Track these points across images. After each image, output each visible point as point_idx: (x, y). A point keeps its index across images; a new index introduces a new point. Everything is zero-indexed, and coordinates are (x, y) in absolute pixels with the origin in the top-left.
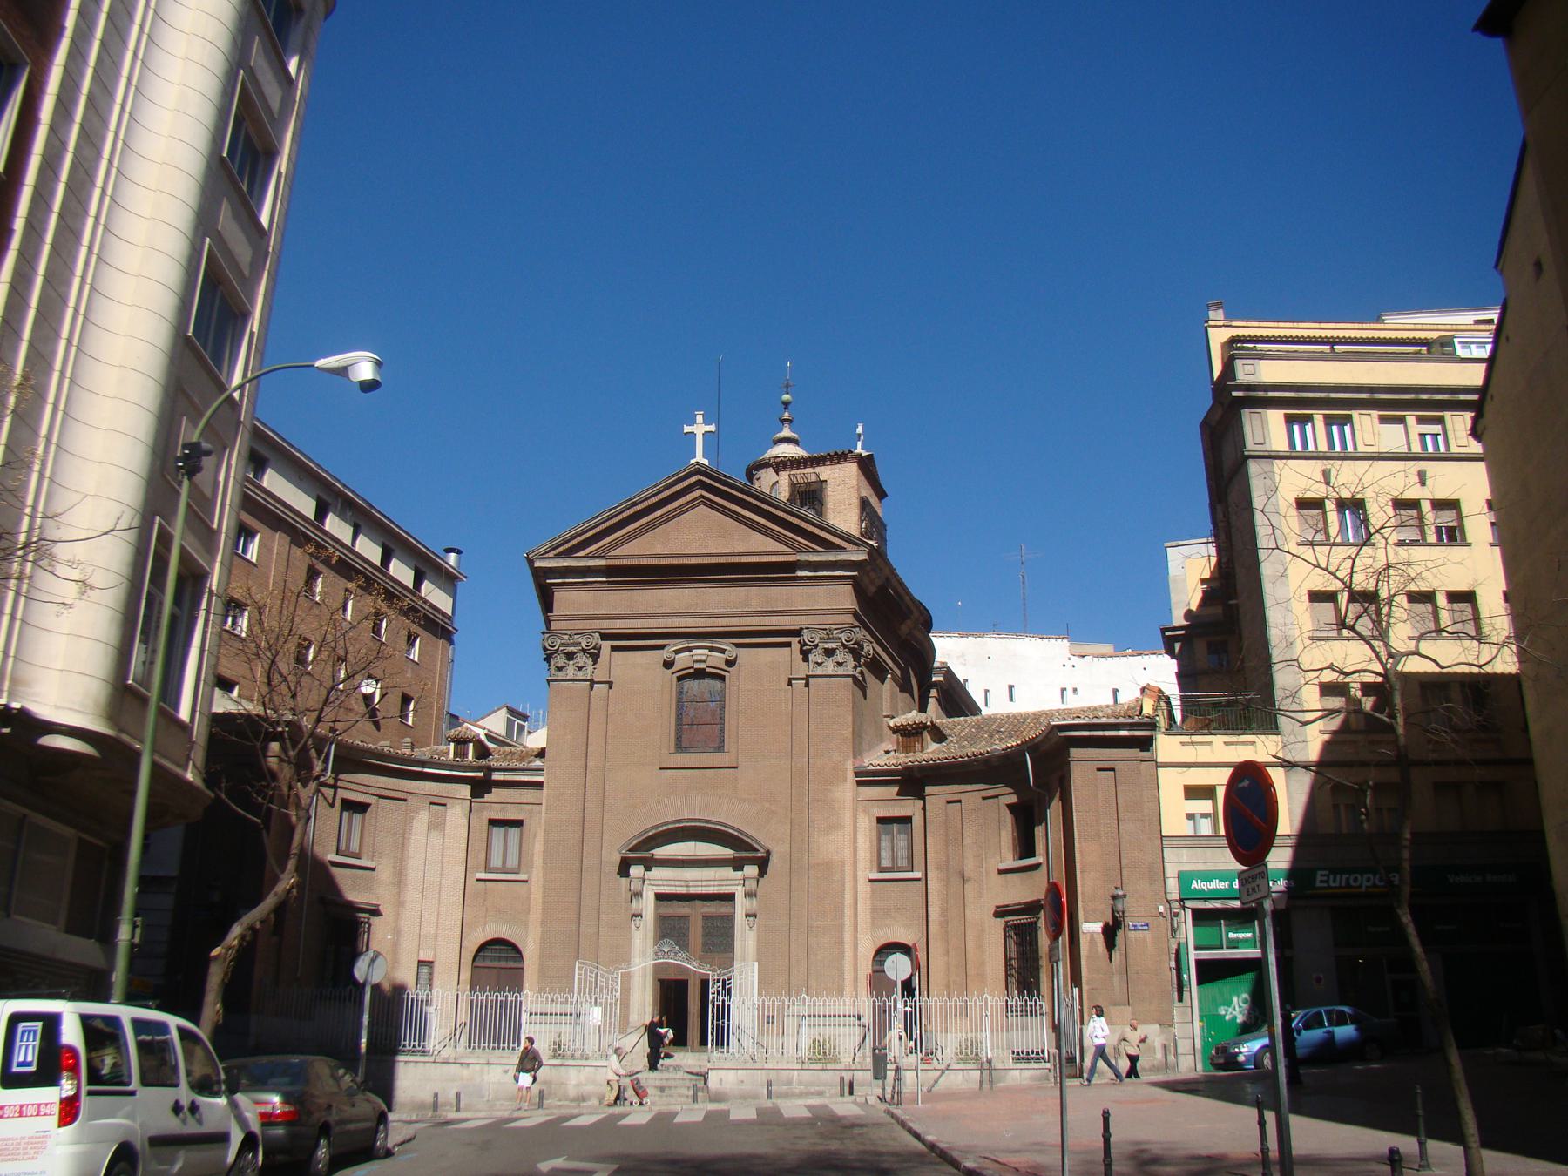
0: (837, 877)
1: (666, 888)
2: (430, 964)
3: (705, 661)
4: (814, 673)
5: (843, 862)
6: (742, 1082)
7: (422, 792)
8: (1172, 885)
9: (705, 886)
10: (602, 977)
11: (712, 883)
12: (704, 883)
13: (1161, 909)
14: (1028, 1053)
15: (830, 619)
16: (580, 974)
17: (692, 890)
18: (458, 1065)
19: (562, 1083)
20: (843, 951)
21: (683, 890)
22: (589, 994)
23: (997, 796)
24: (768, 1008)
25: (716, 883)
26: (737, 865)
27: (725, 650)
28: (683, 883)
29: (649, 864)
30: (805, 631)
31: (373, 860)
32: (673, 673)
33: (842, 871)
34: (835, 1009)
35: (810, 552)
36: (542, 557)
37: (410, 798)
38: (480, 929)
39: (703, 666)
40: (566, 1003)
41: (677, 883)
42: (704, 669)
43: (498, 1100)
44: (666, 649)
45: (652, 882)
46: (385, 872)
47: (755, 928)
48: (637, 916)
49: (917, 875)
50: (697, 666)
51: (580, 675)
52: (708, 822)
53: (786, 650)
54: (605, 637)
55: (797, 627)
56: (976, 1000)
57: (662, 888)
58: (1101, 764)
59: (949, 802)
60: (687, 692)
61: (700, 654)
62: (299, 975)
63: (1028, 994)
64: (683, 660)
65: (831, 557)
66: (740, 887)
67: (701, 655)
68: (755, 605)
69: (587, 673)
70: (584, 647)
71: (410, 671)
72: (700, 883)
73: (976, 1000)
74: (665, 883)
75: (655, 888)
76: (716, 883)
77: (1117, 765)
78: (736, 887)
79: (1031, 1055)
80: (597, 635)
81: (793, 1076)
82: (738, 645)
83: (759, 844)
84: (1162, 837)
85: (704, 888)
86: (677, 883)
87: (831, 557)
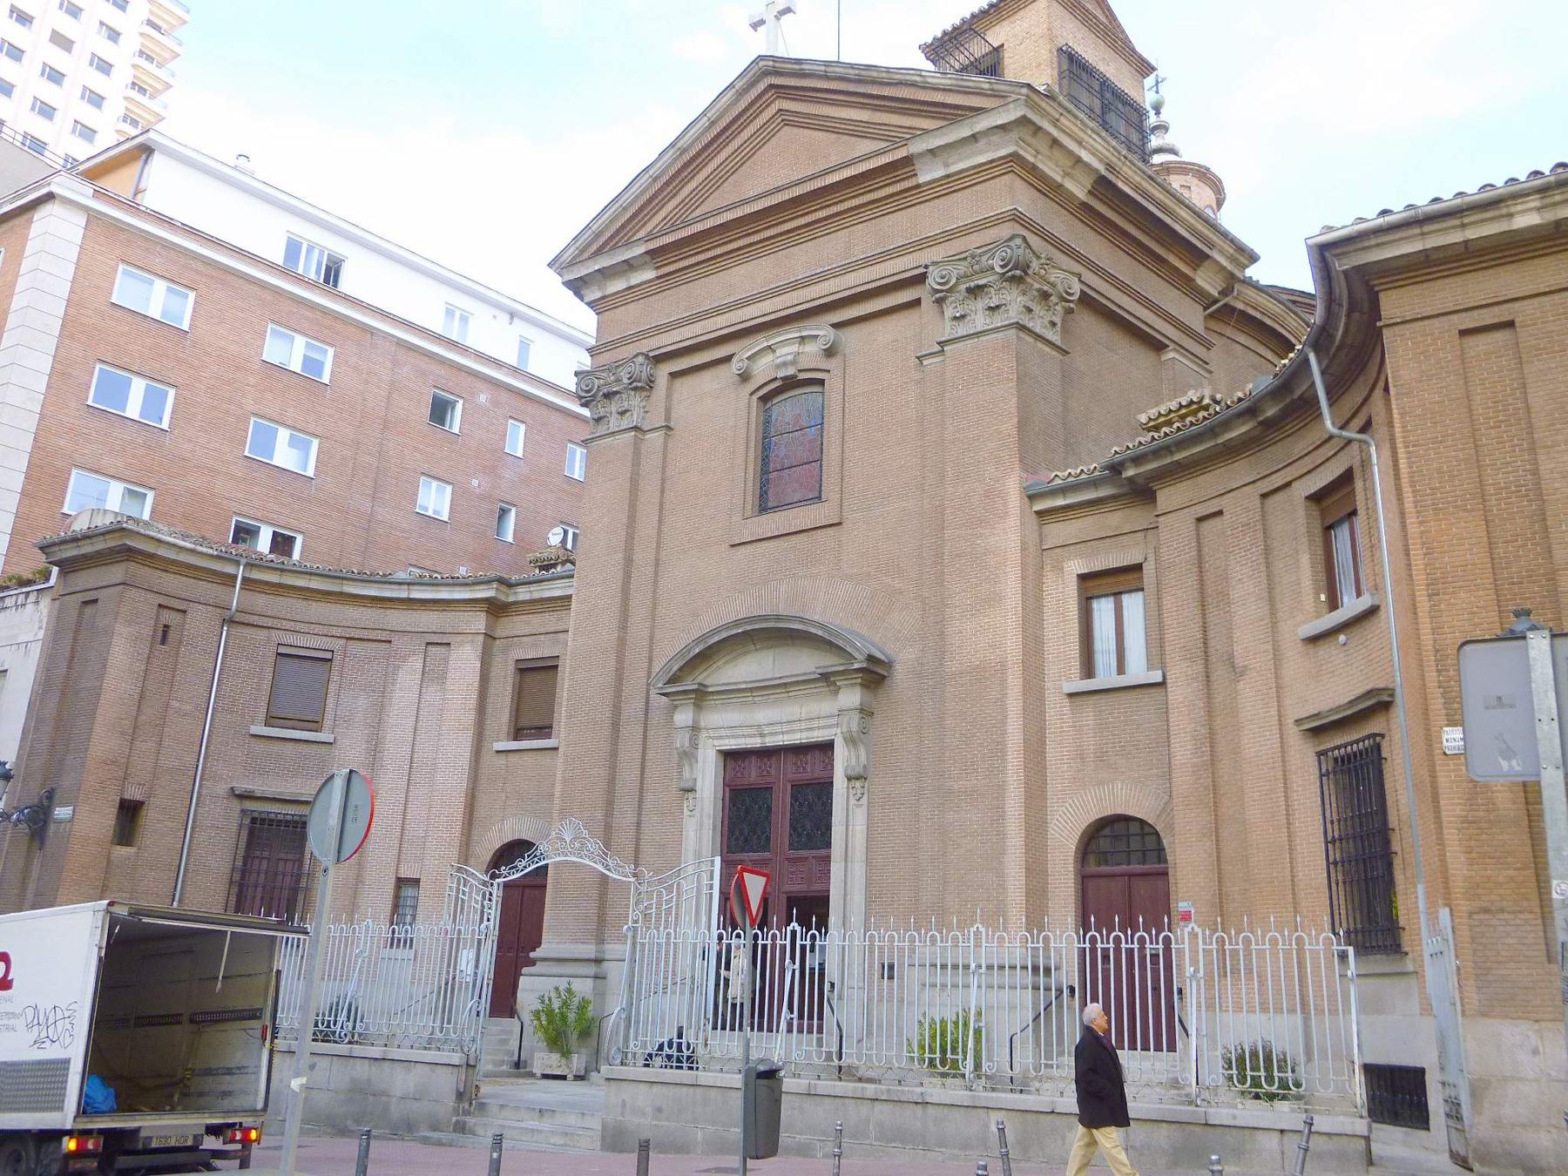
5: (1003, 666)
6: (659, 1110)
9: (788, 732)
11: (796, 726)
20: (1002, 836)
21: (755, 743)
23: (1288, 485)
28: (753, 731)
32: (751, 394)
33: (1003, 682)
37: (395, 638)
38: (495, 828)
39: (791, 371)
42: (793, 377)
44: (735, 360)
50: (781, 374)
56: (872, 936)
58: (1469, 321)
63: (1250, 923)
64: (764, 369)
65: (964, 131)
75: (716, 742)
78: (834, 731)
80: (640, 359)
85: (786, 737)
87: (964, 131)
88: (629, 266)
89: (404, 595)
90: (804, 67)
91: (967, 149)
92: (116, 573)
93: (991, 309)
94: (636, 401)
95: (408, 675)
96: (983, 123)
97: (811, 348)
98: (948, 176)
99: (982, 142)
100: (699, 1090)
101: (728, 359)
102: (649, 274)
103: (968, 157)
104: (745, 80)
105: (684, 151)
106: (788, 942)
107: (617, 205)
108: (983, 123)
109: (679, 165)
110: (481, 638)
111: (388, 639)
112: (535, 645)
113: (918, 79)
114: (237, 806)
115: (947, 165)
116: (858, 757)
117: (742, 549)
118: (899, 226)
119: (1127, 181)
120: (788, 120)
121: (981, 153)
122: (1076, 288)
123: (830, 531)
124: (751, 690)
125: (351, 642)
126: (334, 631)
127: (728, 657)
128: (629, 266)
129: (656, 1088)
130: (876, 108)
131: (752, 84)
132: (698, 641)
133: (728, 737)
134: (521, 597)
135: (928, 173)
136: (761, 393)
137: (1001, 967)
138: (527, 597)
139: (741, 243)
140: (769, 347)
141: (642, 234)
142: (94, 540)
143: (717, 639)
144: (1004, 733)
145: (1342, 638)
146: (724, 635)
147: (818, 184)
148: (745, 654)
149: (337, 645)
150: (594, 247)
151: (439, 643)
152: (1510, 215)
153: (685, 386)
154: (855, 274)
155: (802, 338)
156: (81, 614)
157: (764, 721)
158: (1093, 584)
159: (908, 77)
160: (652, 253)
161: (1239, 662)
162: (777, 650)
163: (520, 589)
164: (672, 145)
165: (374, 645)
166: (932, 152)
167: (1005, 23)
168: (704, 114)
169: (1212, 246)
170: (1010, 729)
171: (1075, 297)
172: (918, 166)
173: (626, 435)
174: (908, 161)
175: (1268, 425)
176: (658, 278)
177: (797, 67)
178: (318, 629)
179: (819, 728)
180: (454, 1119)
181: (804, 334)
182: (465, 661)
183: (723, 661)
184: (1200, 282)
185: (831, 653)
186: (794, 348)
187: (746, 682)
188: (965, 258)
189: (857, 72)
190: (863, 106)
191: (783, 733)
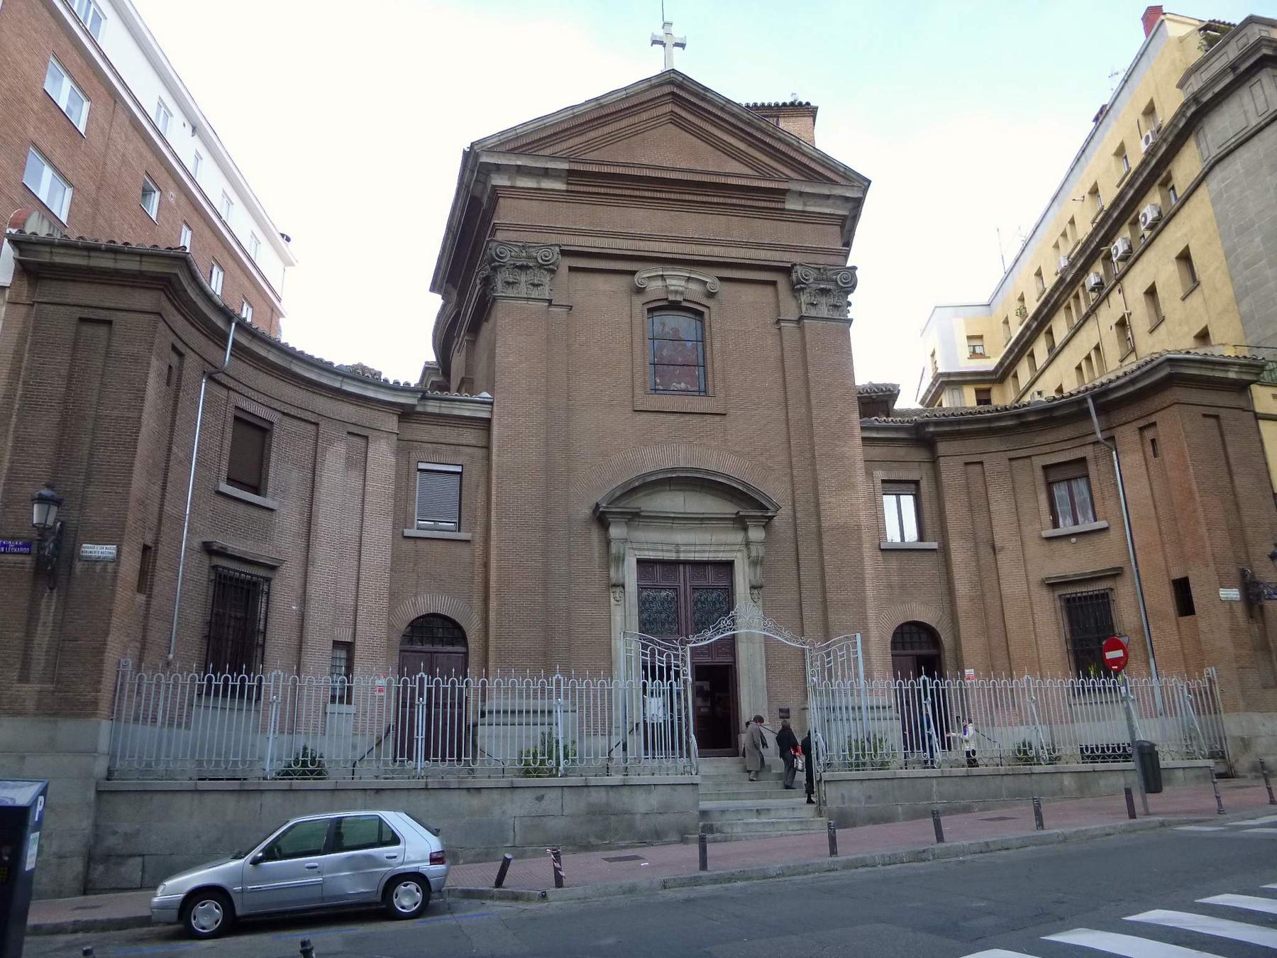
1: (651, 553)
2: (349, 647)
3: (682, 293)
6: (870, 797)
7: (338, 418)
9: (699, 552)
10: (661, 654)
11: (707, 548)
12: (698, 548)
14: (1103, 751)
17: (683, 556)
18: (465, 791)
21: (672, 556)
22: (676, 680)
23: (1029, 457)
26: (741, 523)
29: (634, 517)
30: (798, 267)
33: (860, 538)
36: (490, 151)
39: (679, 298)
40: (528, 697)
41: (665, 548)
43: (531, 844)
44: (637, 276)
47: (760, 603)
48: (615, 586)
49: (934, 545)
50: (671, 298)
51: (535, 293)
52: (707, 472)
53: (769, 290)
54: (564, 253)
57: (646, 553)
59: (967, 464)
61: (675, 284)
62: (171, 656)
64: (655, 288)
65: (825, 190)
66: (739, 555)
67: (677, 283)
68: (736, 236)
70: (540, 261)
72: (693, 548)
74: (649, 546)
75: (637, 553)
77: (1223, 413)
78: (735, 554)
79: (1108, 753)
80: (557, 249)
82: (721, 279)
83: (772, 504)
85: (696, 555)
87: (825, 190)
88: (546, 173)
89: (337, 385)
90: (708, 94)
91: (821, 202)
92: (145, 299)
94: (546, 278)
95: (335, 458)
96: (837, 191)
97: (694, 286)
98: (803, 212)
99: (830, 202)
100: (895, 781)
101: (633, 273)
102: (563, 187)
103: (819, 206)
104: (658, 80)
105: (602, 106)
106: (922, 687)
107: (541, 123)
109: (595, 115)
110: (395, 437)
113: (795, 143)
114: (206, 560)
115: (805, 205)
116: (755, 574)
117: (644, 416)
118: (765, 230)
120: (676, 121)
121: (828, 206)
123: (718, 418)
124: (674, 518)
125: (286, 418)
126: (276, 405)
127: (647, 492)
128: (546, 173)
130: (751, 145)
131: (660, 85)
132: (638, 478)
133: (648, 550)
134: (430, 409)
135: (792, 205)
138: (437, 411)
140: (662, 275)
141: (548, 152)
142: (120, 257)
143: (654, 478)
144: (863, 569)
145: (1073, 540)
146: (661, 476)
147: (723, 180)
148: (662, 491)
150: (512, 145)
151: (361, 435)
152: (1228, 371)
153: (581, 278)
155: (689, 278)
156: (77, 333)
157: (680, 542)
159: (789, 139)
160: (571, 172)
161: (998, 544)
162: (687, 493)
163: (431, 403)
164: (596, 99)
165: (303, 424)
166: (801, 194)
168: (625, 89)
172: (788, 197)
173: (541, 304)
174: (784, 192)
175: (1022, 424)
176: (567, 191)
177: (703, 92)
178: (264, 399)
179: (723, 551)
180: (701, 824)
181: (693, 276)
182: (382, 454)
183: (641, 494)
185: (731, 502)
186: (683, 283)
187: (674, 513)
189: (751, 118)
190: (743, 140)
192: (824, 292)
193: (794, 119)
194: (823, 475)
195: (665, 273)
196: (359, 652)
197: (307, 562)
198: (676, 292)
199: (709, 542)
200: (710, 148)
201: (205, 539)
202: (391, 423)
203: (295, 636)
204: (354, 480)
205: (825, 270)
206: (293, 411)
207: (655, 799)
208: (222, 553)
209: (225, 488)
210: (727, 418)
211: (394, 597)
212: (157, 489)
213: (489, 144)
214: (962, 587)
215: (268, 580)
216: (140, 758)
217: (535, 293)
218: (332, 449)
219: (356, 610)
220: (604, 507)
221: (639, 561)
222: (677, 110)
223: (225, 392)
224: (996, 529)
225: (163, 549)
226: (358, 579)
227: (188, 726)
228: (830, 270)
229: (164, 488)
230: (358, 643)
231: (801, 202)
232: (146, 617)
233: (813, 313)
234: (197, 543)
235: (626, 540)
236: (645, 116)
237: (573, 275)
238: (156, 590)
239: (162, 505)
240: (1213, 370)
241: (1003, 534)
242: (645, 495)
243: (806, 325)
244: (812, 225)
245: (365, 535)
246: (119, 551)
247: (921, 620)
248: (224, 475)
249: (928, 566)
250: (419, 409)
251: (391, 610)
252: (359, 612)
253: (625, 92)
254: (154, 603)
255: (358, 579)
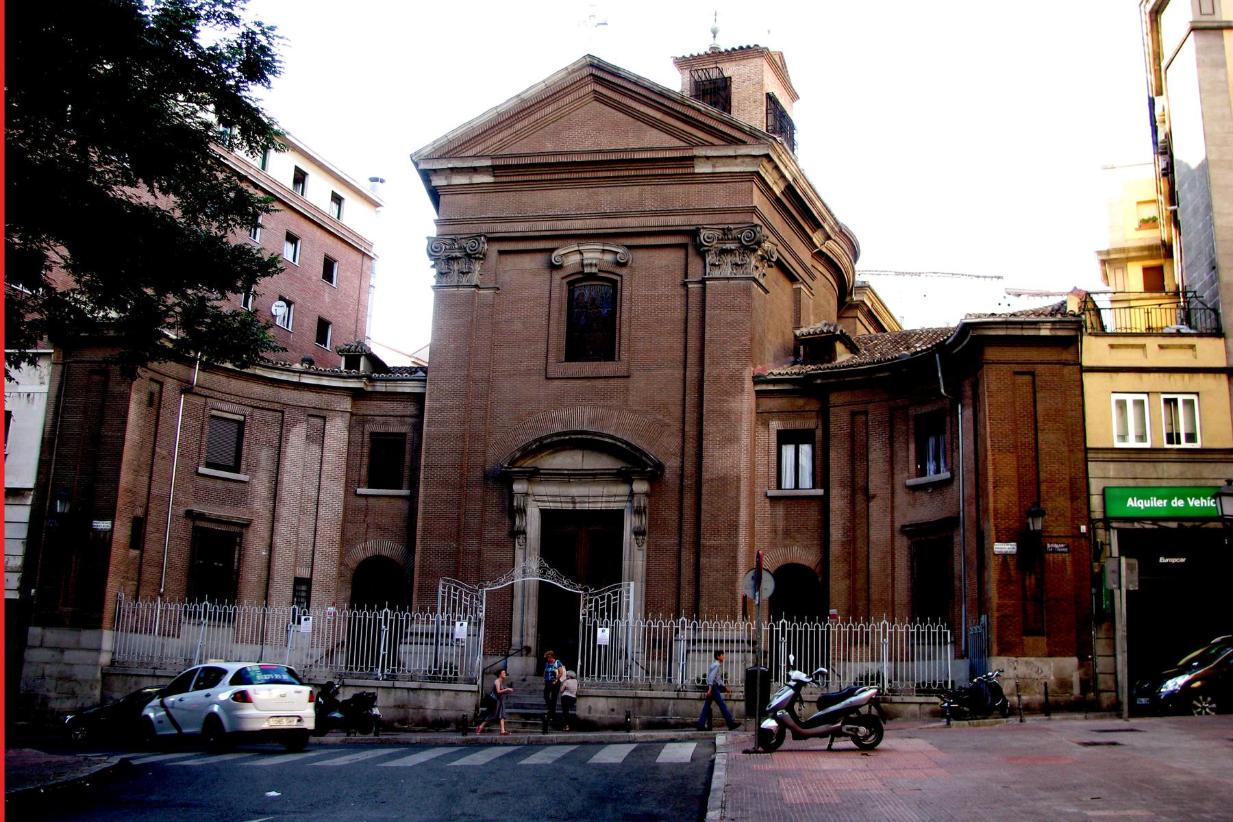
0: (732, 494)
1: (552, 504)
3: (596, 265)
4: (711, 276)
5: (738, 478)
6: (613, 710)
8: (1096, 501)
10: (466, 595)
11: (599, 499)
12: (591, 499)
13: (1083, 529)
15: (729, 218)
16: (444, 592)
19: (421, 708)
22: (442, 614)
24: (655, 633)
25: (604, 499)
26: (623, 477)
27: (617, 253)
28: (569, 499)
29: (534, 475)
31: (246, 474)
32: (563, 278)
33: (738, 488)
34: (727, 634)
35: (705, 145)
39: (594, 270)
41: (563, 499)
44: (555, 253)
45: (537, 498)
46: (261, 486)
47: (645, 547)
50: (587, 270)
51: (464, 281)
54: (490, 240)
55: (694, 228)
57: (548, 504)
60: (578, 298)
62: (162, 590)
68: (649, 204)
69: (475, 278)
71: (327, 295)
72: (587, 500)
73: (695, 624)
74: (550, 498)
75: (539, 504)
76: (604, 499)
77: (1040, 369)
81: (669, 705)
82: (630, 248)
84: (1086, 450)
85: (591, 505)
86: (563, 499)
88: (475, 170)
89: (296, 379)
93: (737, 265)
95: (297, 437)
97: (609, 257)
99: (739, 160)
103: (728, 166)
105: (523, 101)
108: (743, 150)
110: (348, 415)
111: (282, 409)
112: (384, 423)
118: (678, 194)
119: (800, 187)
120: (599, 98)
122: (776, 255)
123: (621, 381)
125: (256, 410)
126: (247, 402)
127: (549, 452)
128: (475, 170)
129: (610, 700)
133: (549, 501)
136: (569, 279)
137: (732, 641)
138: (383, 389)
139: (564, 176)
140: (579, 250)
144: (738, 516)
147: (629, 156)
149: (248, 410)
151: (320, 416)
153: (510, 261)
154: (646, 218)
157: (576, 494)
158: (785, 437)
161: (872, 491)
163: (378, 384)
164: (518, 96)
166: (708, 158)
167: (734, 63)
169: (824, 220)
170: (741, 514)
171: (774, 260)
172: (696, 161)
174: (692, 158)
178: (235, 399)
179: (614, 502)
181: (606, 248)
182: (337, 430)
184: (814, 240)
186: (598, 255)
188: (723, 229)
190: (658, 110)
191: (589, 502)
192: (724, 252)
193: (745, 61)
194: (708, 428)
195: (581, 248)
196: (315, 586)
197: (274, 519)
198: (591, 265)
199: (601, 494)
200: (631, 119)
201: (189, 508)
202: (346, 404)
203: (264, 574)
204: (314, 451)
205: (729, 230)
206: (262, 404)
207: (443, 699)
208: (201, 516)
209: (202, 470)
210: (631, 379)
211: (346, 541)
212: (145, 479)
213: (425, 152)
214: (836, 533)
215: (241, 535)
216: (139, 655)
217: (464, 281)
218: (295, 431)
219: (313, 555)
220: (506, 468)
221: (543, 512)
222: (599, 89)
223: (203, 400)
224: (871, 477)
225: (152, 518)
226: (316, 529)
227: (178, 637)
228: (735, 229)
229: (150, 478)
230: (314, 579)
231: (710, 165)
232: (141, 565)
233: (716, 273)
234: (182, 511)
235: (527, 494)
236: (567, 99)
237: (503, 258)
238: (147, 547)
239: (149, 488)
240: (1022, 329)
241: (876, 482)
242: (548, 454)
243: (708, 286)
244: (725, 185)
245: (321, 495)
246: (113, 525)
247: (801, 562)
248: (203, 461)
249: (813, 512)
250: (369, 389)
251: (342, 555)
252: (316, 556)
253: (544, 84)
254: (145, 555)
255: (316, 529)
